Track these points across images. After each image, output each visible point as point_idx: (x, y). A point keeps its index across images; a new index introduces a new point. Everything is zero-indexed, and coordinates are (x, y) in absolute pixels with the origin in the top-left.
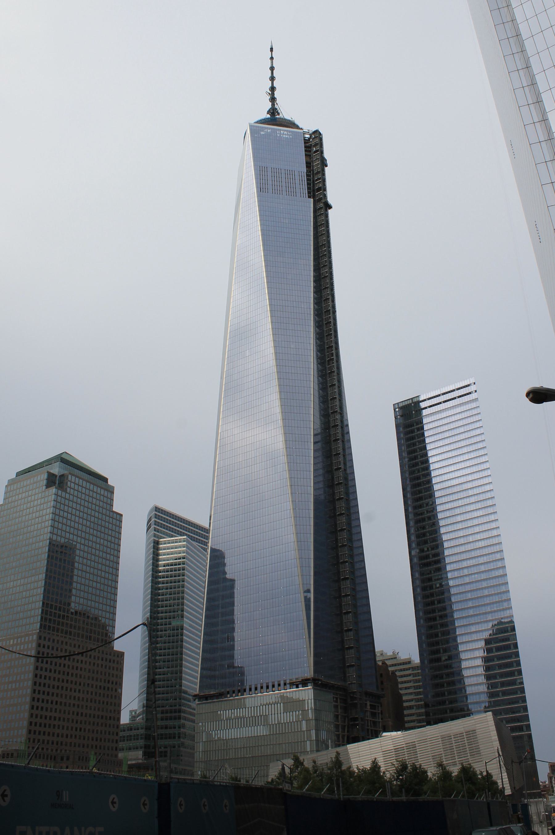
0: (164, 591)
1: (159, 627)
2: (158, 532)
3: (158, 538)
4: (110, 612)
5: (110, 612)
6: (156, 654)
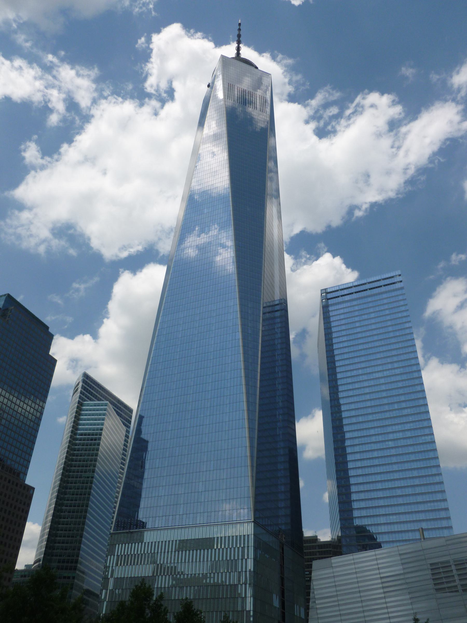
0: (80, 447)
1: (70, 479)
2: (83, 395)
3: (82, 400)
4: (24, 459)
5: (24, 459)
6: (61, 511)
